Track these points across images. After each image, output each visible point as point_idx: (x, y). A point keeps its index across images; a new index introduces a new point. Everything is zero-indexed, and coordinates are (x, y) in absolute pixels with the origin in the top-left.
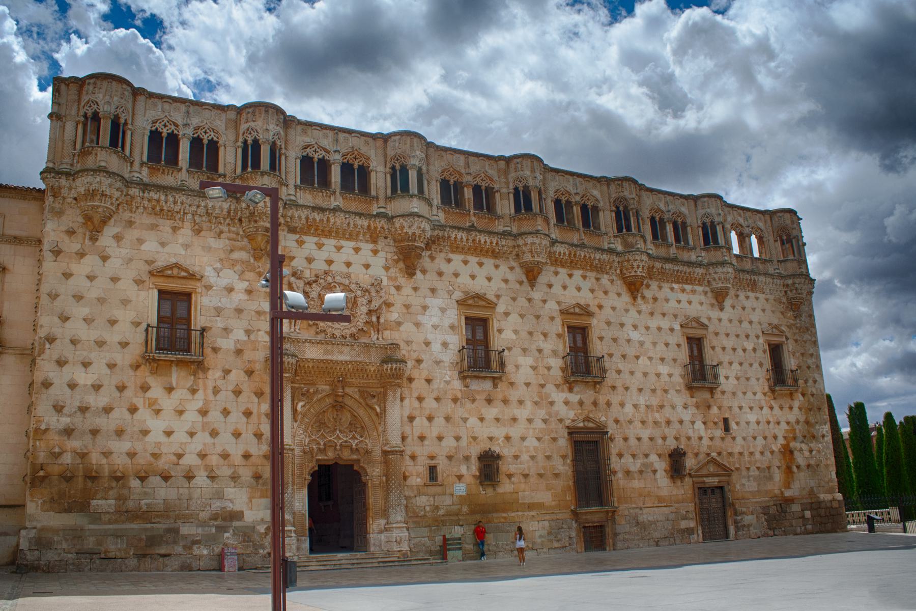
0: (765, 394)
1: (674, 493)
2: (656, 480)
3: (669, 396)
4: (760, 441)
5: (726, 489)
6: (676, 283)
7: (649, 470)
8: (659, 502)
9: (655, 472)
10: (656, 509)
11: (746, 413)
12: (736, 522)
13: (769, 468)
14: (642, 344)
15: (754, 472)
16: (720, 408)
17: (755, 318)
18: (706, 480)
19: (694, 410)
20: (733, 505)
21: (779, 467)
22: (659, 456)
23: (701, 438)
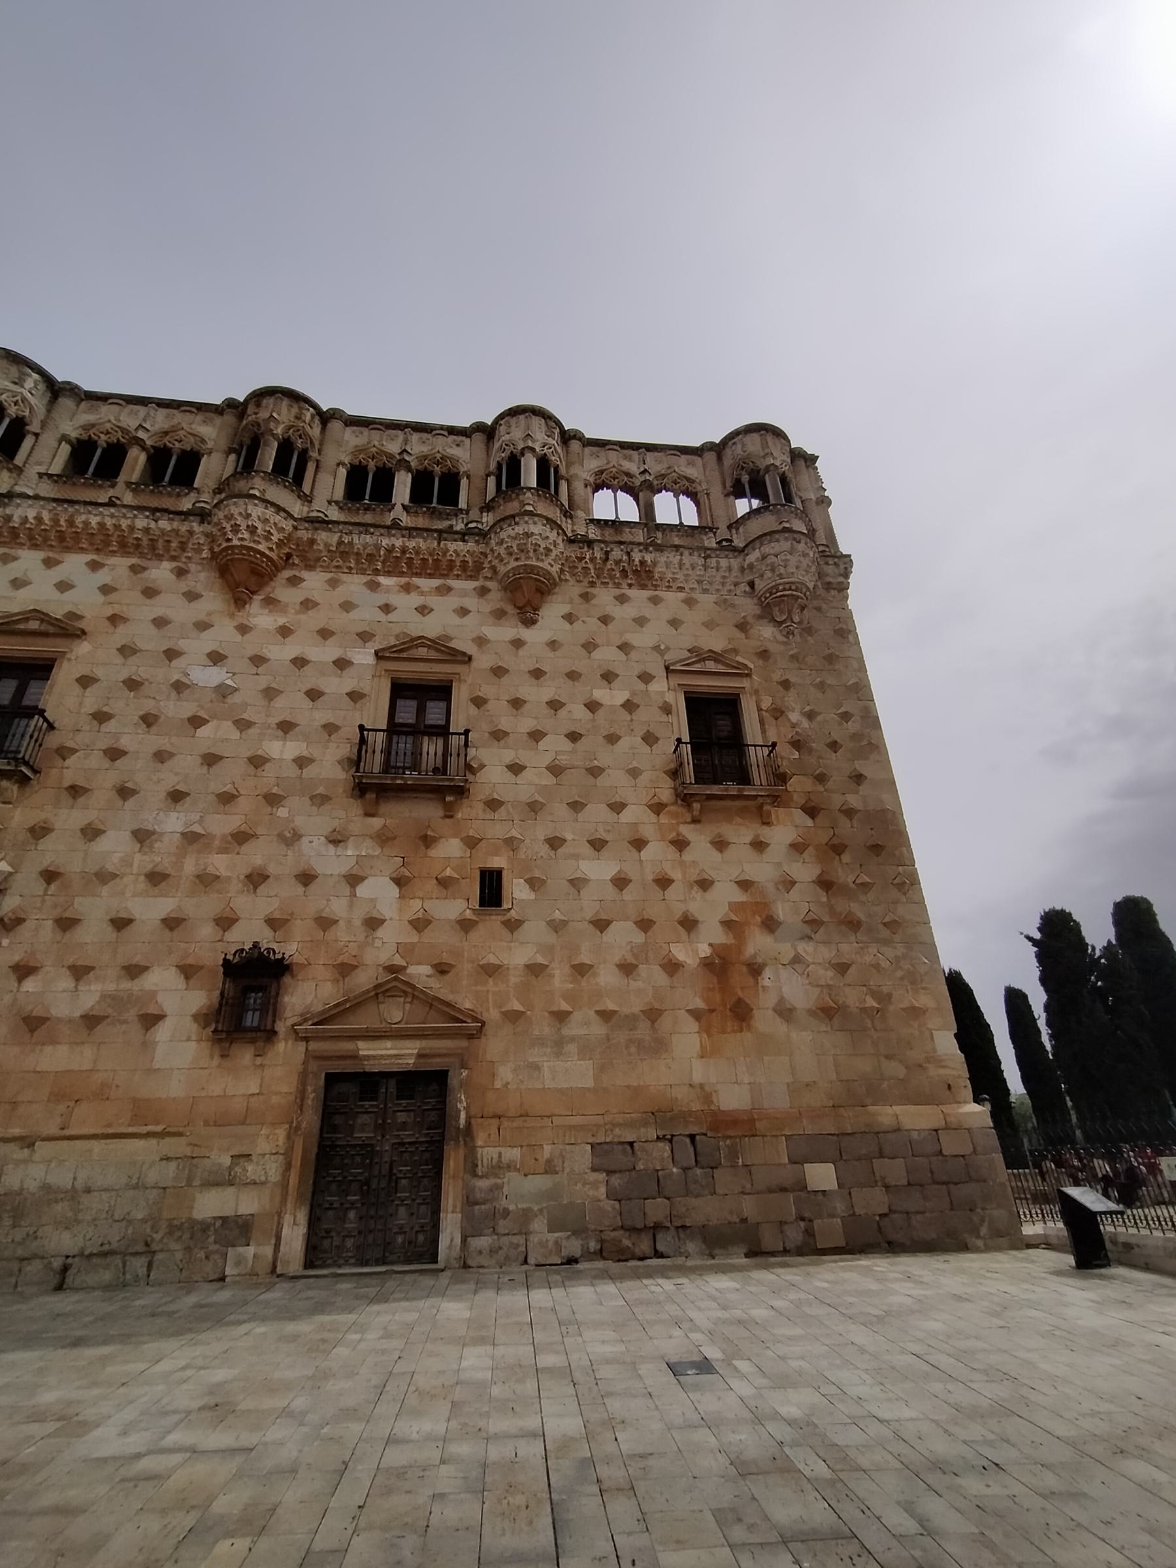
0: (658, 808)
1: (216, 1089)
2: (147, 1047)
3: (282, 812)
4: (623, 936)
5: (453, 1081)
6: (388, 574)
7: (131, 1014)
8: (136, 1119)
9: (151, 1020)
10: (97, 1146)
11: (576, 857)
12: (470, 1202)
13: (653, 1015)
14: (223, 692)
15: (584, 1025)
16: (472, 843)
17: (642, 639)
18: (365, 1048)
19: (368, 848)
20: (469, 1131)
21: (696, 1014)
22: (188, 971)
23: (373, 923)
